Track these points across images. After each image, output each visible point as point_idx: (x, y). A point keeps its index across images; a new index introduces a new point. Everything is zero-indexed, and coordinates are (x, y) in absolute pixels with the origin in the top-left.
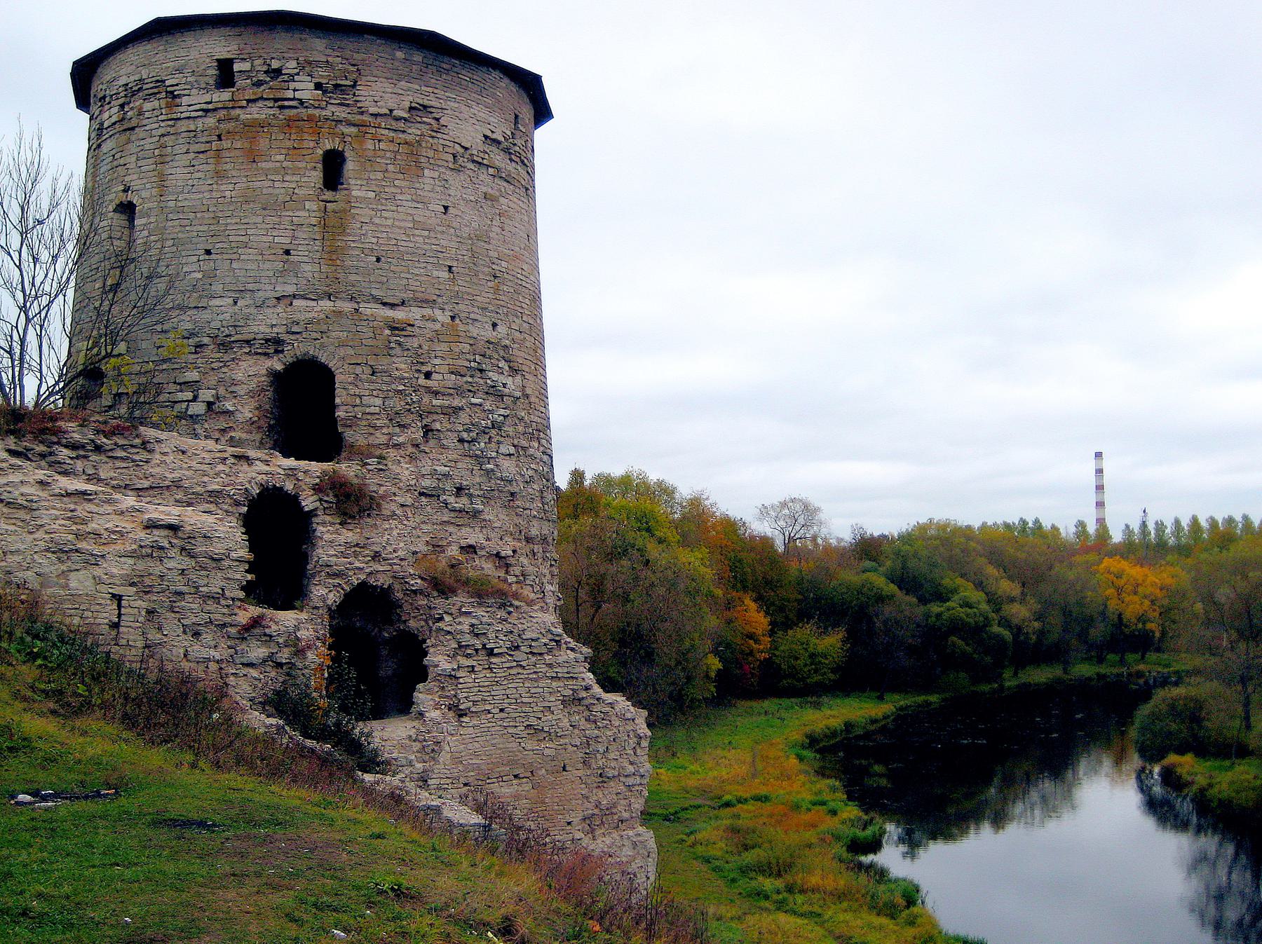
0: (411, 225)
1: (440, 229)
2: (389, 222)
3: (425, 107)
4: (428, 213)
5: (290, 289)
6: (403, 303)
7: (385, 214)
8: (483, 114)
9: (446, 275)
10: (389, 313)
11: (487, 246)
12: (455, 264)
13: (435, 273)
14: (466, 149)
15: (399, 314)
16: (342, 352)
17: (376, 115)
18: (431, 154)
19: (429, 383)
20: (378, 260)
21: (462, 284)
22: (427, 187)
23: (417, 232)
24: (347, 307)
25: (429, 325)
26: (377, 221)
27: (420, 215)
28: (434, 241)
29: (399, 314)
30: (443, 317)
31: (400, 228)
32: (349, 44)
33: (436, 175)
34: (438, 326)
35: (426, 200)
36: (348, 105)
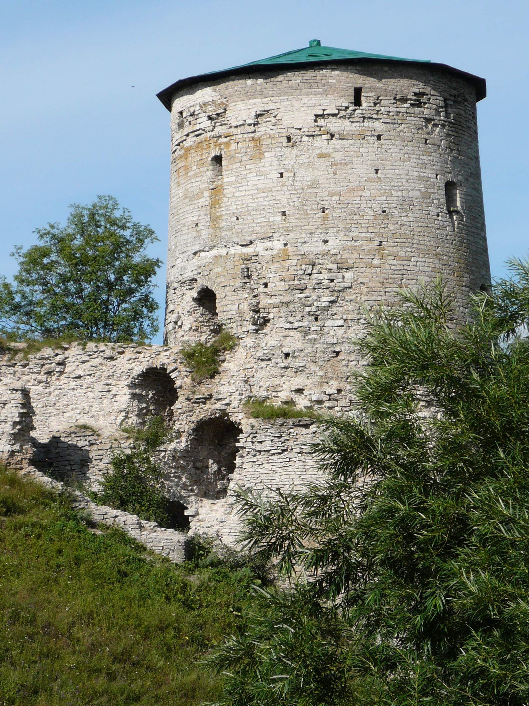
0: (256, 191)
1: (275, 189)
2: (243, 193)
3: (268, 111)
4: (266, 181)
5: (197, 248)
6: (251, 243)
7: (241, 189)
8: (314, 100)
9: (279, 218)
10: (244, 250)
11: (316, 190)
12: (286, 209)
13: (272, 219)
14: (300, 129)
15: (250, 250)
16: (219, 280)
17: (237, 127)
18: (269, 141)
19: (266, 290)
20: (238, 219)
21: (292, 221)
22: (267, 164)
23: (259, 195)
24: (223, 251)
25: (269, 252)
26: (236, 194)
27: (262, 183)
28: (271, 198)
29: (250, 250)
30: (278, 245)
31: (248, 195)
32: (300, 52)
33: (273, 154)
34: (275, 252)
35: (265, 173)
36: (225, 124)
